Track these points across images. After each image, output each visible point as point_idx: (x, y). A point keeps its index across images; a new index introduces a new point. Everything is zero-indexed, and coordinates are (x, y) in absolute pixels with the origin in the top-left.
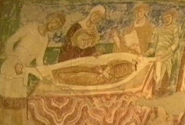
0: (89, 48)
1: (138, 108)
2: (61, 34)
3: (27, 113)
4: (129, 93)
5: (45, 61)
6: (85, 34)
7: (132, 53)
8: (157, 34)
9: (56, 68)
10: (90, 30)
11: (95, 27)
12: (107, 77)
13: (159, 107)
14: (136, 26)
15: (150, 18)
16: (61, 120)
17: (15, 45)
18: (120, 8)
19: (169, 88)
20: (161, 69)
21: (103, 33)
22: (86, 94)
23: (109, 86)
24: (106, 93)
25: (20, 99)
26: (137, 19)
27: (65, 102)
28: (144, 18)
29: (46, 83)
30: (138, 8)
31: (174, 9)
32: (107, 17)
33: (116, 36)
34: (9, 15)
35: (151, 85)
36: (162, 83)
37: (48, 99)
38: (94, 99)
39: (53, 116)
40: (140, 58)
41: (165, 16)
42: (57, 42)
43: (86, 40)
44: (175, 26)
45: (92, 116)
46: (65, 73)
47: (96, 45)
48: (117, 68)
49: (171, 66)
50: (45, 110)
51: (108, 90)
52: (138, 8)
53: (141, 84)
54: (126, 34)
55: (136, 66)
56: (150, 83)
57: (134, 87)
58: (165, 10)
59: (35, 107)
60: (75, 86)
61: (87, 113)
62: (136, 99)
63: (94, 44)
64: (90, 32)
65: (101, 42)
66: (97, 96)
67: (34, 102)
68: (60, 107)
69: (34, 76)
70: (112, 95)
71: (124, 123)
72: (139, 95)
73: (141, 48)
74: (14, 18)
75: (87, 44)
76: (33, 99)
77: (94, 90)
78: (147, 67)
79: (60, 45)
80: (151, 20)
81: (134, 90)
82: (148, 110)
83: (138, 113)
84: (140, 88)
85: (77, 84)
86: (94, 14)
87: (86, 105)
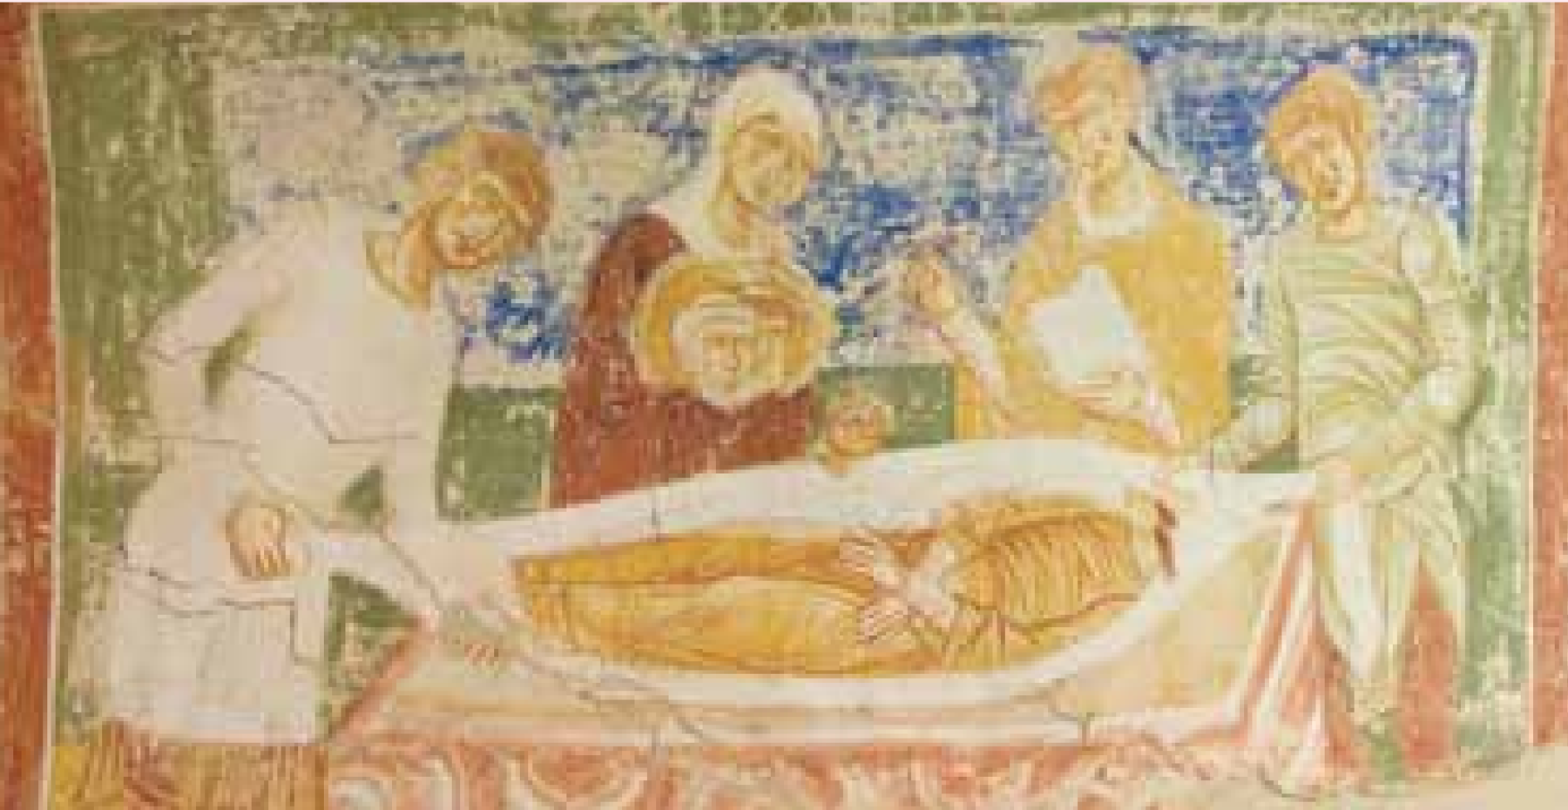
7: (1112, 439)
10: (747, 263)
11: (786, 243)
12: (945, 622)
14: (1093, 227)
15: (1183, 167)
20: (1377, 559)
26: (1088, 175)
28: (1140, 167)
29: (468, 648)
32: (845, 164)
34: (134, 144)
49: (1457, 538)
55: (1163, 541)
63: (805, 377)
69: (374, 594)
78: (1257, 553)
80: (1190, 178)
86: (747, 141)
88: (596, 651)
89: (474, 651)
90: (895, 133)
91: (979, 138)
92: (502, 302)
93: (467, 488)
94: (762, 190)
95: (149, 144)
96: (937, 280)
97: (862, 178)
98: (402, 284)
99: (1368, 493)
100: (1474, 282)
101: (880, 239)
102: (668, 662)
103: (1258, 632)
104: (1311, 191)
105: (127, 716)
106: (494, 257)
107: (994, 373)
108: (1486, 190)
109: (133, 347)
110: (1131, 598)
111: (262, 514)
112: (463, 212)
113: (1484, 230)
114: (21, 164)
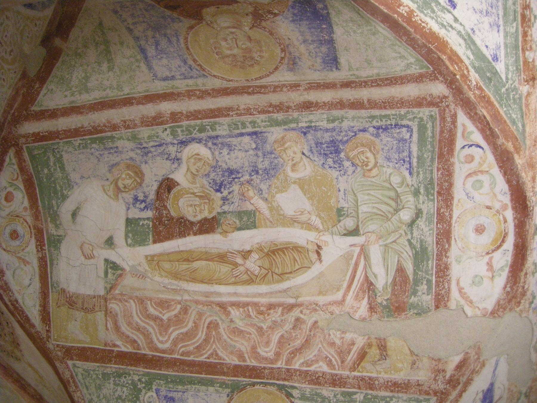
0: (206, 219)
1: (336, 337)
2: (146, 197)
3: (106, 320)
4: (311, 304)
5: (130, 241)
6: (193, 196)
8: (350, 189)
9: (152, 253)
10: (196, 188)
11: (206, 183)
12: (256, 273)
13: (390, 339)
14: (293, 175)
16: (167, 337)
17: (74, 215)
18: (240, 144)
19: (413, 299)
20: (384, 259)
21: (225, 193)
22: (212, 299)
23: (264, 288)
24: (256, 300)
25: (95, 297)
26: (290, 163)
27: (173, 310)
29: (136, 275)
30: (282, 141)
31: (367, 135)
32: (220, 163)
33: (256, 197)
34: (49, 170)
35: (364, 292)
36: (393, 290)
37: (141, 301)
38: (230, 309)
39: (151, 330)
40: (323, 238)
41: (355, 152)
42: (142, 210)
43: (195, 205)
44: (389, 171)
45: (228, 340)
46: (170, 261)
47: (219, 213)
48: (275, 255)
49: (411, 255)
50: (136, 318)
51: (260, 295)
52: (282, 141)
53: (338, 289)
54: (276, 193)
56: (360, 289)
57: (320, 293)
58: (345, 139)
59: (119, 313)
60: (191, 283)
61: (218, 333)
62: (328, 316)
64: (199, 192)
65: (226, 208)
66: (233, 304)
67: (116, 303)
68: (165, 318)
69: (114, 263)
70: (271, 306)
71: (298, 360)
72: (336, 310)
73: (319, 216)
74: (59, 174)
75: (200, 212)
76: (116, 299)
77: (229, 294)
78: (347, 257)
79: (149, 214)
80: (322, 162)
81: (322, 300)
82: (360, 342)
83: (333, 344)
84: (339, 296)
85: (194, 280)
86: (192, 160)
87: (215, 318)
88: (166, 277)
89: (138, 276)
90: (233, 155)
91: (257, 155)
92: (136, 199)
93: (132, 240)
94: (198, 171)
95: (52, 170)
96: (248, 190)
97: (224, 165)
98: (112, 196)
99: (381, 242)
100: (416, 186)
101: (231, 181)
102: (184, 280)
103: (348, 278)
104: (360, 164)
105: (65, 287)
106: (133, 189)
107: (267, 212)
108: (418, 162)
109: (56, 212)
110: (309, 268)
111: (88, 246)
112: (124, 179)
113: (418, 173)
114: (28, 175)
